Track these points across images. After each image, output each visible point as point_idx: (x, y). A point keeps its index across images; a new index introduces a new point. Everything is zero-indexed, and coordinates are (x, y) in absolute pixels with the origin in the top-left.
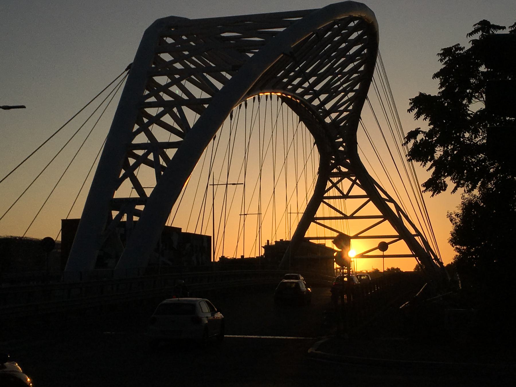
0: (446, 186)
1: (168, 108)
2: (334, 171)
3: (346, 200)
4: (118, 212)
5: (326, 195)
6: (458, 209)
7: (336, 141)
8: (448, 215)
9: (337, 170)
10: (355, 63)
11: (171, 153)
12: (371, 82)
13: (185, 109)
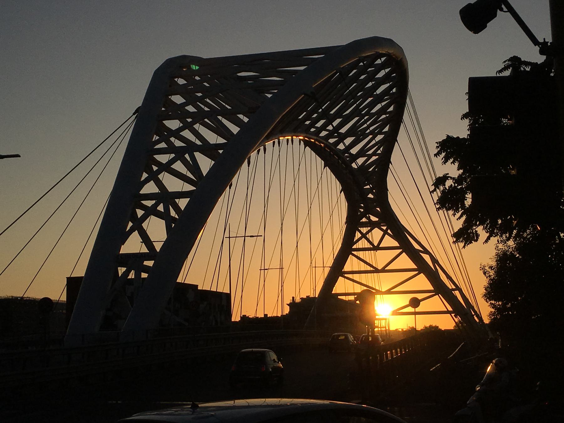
0: (478, 236)
1: (179, 154)
2: (363, 221)
3: (376, 251)
4: (124, 269)
5: (354, 247)
7: (364, 187)
8: (481, 267)
9: (366, 219)
10: (383, 104)
11: (183, 203)
12: (402, 123)
13: (198, 155)
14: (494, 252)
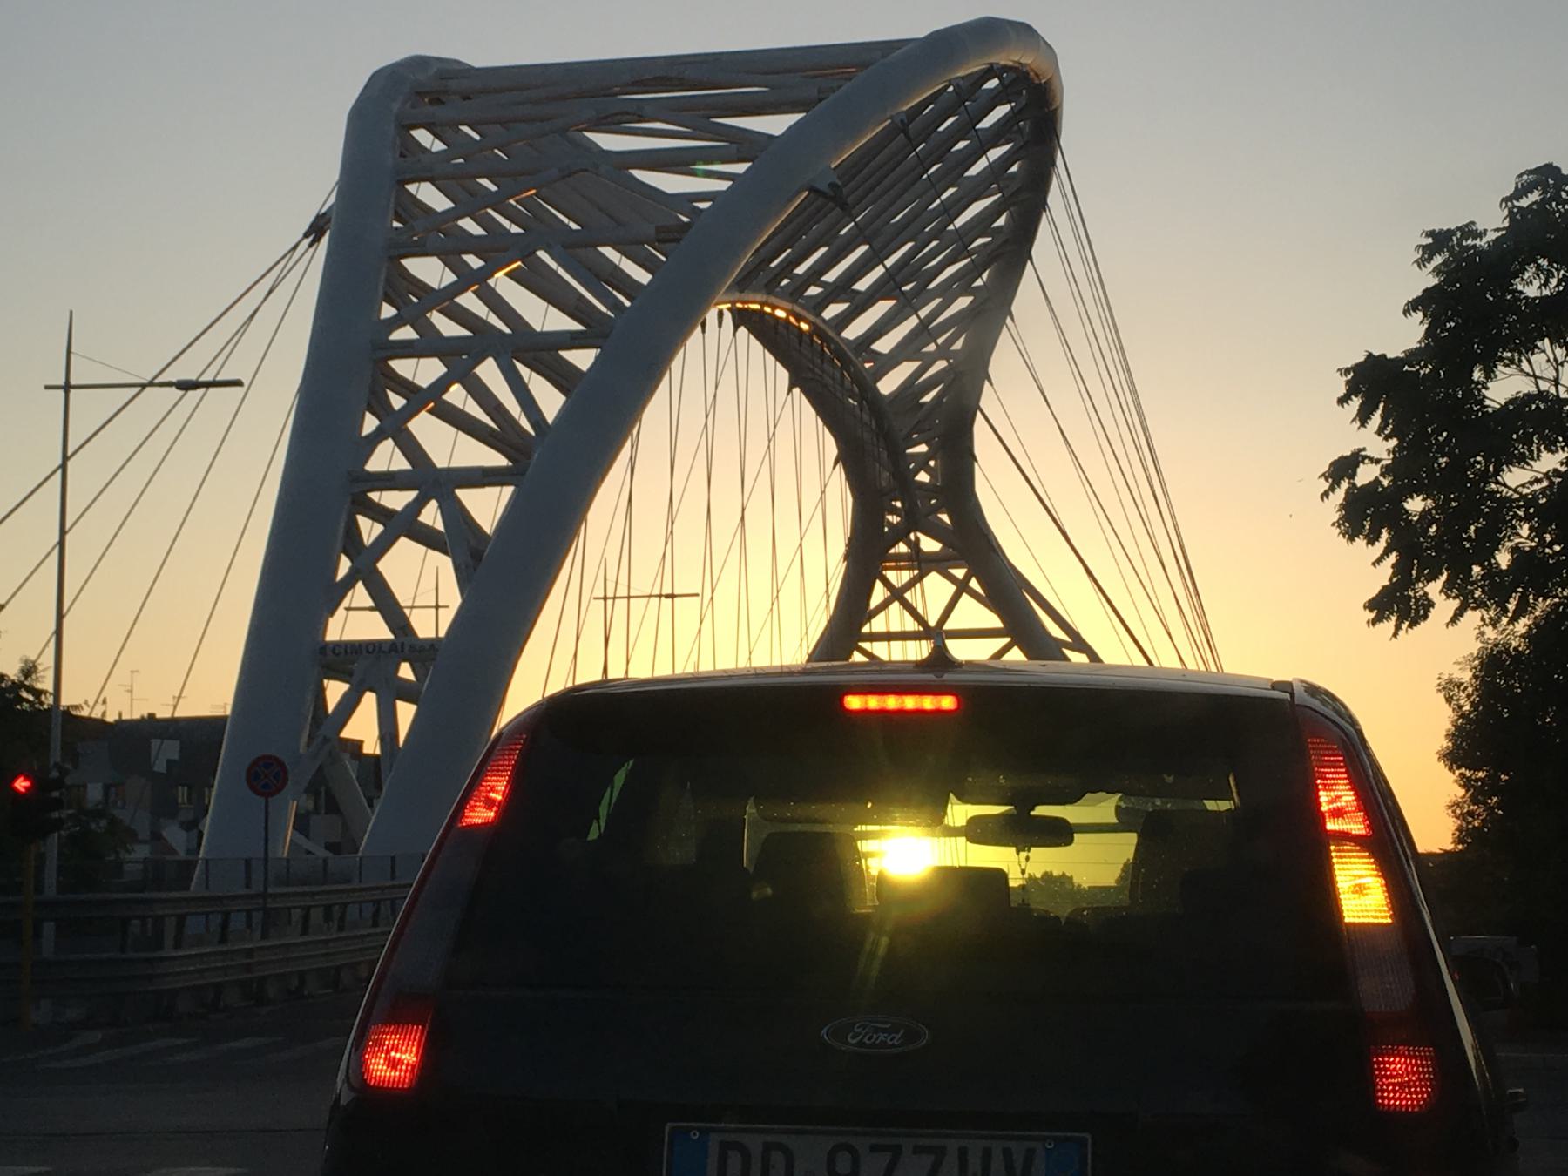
4: (344, 687)
5: (866, 629)
6: (1460, 669)
7: (909, 451)
8: (1439, 685)
12: (1029, 263)
14: (1475, 647)
